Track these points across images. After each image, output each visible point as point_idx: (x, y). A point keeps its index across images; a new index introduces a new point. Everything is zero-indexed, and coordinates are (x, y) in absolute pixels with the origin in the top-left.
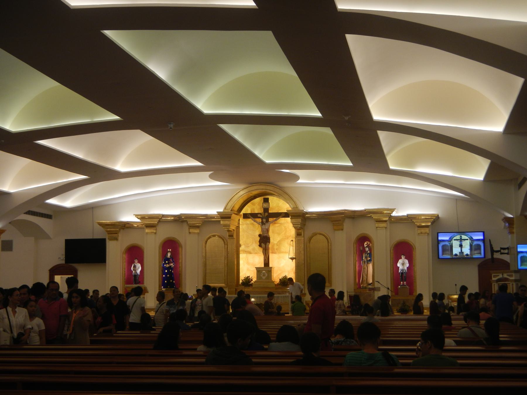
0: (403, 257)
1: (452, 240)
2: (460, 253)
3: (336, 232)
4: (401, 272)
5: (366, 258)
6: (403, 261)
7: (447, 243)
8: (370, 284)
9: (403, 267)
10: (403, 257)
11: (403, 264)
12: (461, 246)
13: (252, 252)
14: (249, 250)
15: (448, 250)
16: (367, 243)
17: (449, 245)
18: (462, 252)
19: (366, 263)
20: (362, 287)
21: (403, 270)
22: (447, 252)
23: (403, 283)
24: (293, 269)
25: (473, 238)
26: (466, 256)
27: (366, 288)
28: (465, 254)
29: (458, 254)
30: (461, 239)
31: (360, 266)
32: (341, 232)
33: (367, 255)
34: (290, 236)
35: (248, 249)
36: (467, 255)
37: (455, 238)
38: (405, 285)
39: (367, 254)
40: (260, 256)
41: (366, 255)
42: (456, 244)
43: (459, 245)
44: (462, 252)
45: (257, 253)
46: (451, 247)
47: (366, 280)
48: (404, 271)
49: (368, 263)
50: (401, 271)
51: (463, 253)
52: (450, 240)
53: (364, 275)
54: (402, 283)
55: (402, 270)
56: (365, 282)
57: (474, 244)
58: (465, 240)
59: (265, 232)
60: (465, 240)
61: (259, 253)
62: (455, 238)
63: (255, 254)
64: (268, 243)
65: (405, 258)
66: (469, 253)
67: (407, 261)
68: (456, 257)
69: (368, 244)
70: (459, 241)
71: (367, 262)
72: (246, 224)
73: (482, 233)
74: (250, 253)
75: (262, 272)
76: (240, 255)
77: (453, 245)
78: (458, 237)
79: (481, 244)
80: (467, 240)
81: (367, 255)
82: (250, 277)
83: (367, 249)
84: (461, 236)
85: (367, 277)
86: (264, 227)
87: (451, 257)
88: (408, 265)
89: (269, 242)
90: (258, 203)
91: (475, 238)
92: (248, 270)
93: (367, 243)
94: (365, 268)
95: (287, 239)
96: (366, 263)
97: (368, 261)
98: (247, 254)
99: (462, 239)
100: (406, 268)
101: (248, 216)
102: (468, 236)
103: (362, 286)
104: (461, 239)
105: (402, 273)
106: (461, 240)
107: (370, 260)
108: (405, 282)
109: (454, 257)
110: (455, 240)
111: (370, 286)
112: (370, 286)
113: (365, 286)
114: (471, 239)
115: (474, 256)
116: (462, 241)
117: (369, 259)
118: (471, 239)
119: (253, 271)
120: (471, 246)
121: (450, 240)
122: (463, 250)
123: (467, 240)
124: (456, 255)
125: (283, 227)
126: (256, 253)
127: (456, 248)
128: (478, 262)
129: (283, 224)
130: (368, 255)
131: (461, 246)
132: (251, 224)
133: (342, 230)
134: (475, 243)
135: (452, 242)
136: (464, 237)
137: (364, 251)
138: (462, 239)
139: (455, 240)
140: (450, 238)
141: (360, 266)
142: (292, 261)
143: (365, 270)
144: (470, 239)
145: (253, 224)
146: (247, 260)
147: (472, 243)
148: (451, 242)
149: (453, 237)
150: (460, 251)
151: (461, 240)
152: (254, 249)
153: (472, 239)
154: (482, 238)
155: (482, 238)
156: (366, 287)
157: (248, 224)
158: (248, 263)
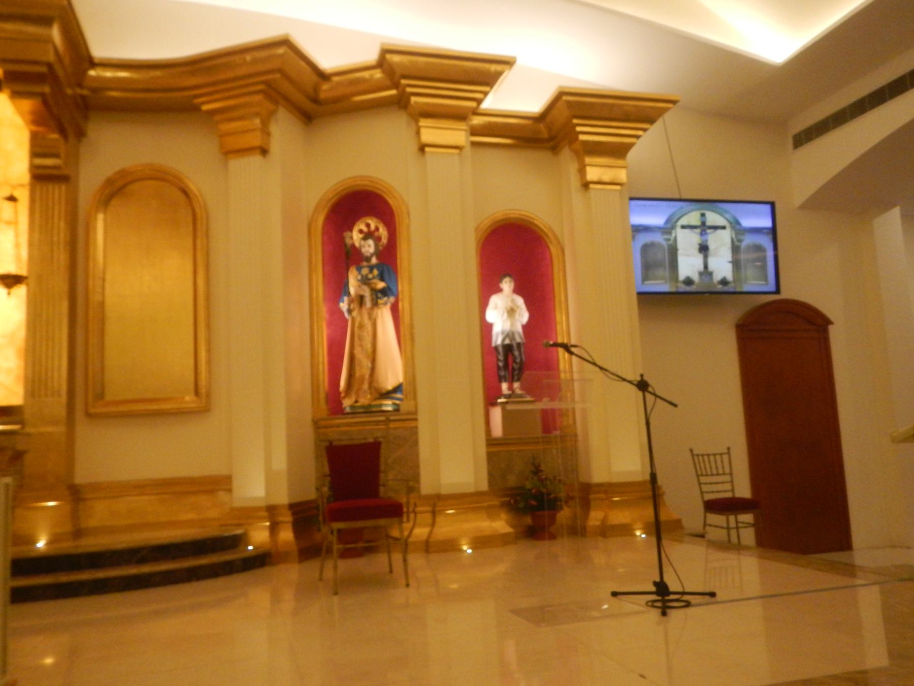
0: (507, 285)
1: (673, 227)
2: (701, 274)
3: (237, 165)
4: (507, 342)
5: (365, 281)
6: (513, 301)
7: (659, 238)
8: (387, 395)
9: (512, 325)
10: (507, 285)
11: (511, 312)
12: (704, 249)
15: (658, 265)
17: (665, 244)
18: (706, 272)
19: (368, 303)
20: (352, 407)
21: (513, 334)
22: (660, 272)
23: (510, 388)
25: (738, 223)
26: (720, 286)
27: (368, 410)
28: (717, 277)
29: (696, 278)
30: (703, 223)
31: (338, 322)
32: (256, 160)
33: (371, 271)
36: (724, 282)
37: (684, 221)
38: (520, 396)
39: (371, 268)
41: (365, 271)
42: (687, 241)
43: (697, 247)
44: (706, 272)
46: (673, 251)
47: (367, 376)
48: (518, 340)
49: (375, 304)
50: (504, 340)
51: (711, 274)
52: (668, 229)
53: (358, 351)
54: (504, 386)
55: (510, 335)
56: (366, 386)
57: (744, 245)
58: (715, 228)
60: (715, 228)
62: (684, 221)
65: (518, 290)
66: (729, 277)
67: (520, 301)
68: (688, 289)
69: (373, 227)
70: (698, 231)
71: (372, 300)
73: (767, 208)
77: (680, 245)
78: (693, 218)
79: (766, 242)
80: (724, 228)
81: (371, 271)
83: (369, 248)
84: (703, 215)
85: (374, 361)
87: (673, 290)
88: (524, 317)
91: (748, 222)
93: (368, 225)
94: (361, 326)
96: (368, 303)
97: (379, 295)
99: (709, 223)
100: (520, 329)
102: (727, 216)
103: (347, 403)
104: (703, 223)
105: (508, 349)
106: (704, 228)
107: (385, 292)
108: (516, 385)
109: (683, 288)
110: (683, 227)
111: (388, 405)
112: (388, 405)
113: (364, 400)
114: (735, 224)
115: (746, 288)
116: (709, 231)
117: (381, 285)
118: (735, 224)
120: (735, 249)
121: (668, 229)
122: (713, 263)
123: (724, 228)
124: (689, 281)
127: (688, 255)
128: (734, 313)
130: (376, 272)
131: (704, 249)
133: (264, 151)
134: (748, 240)
135: (673, 235)
136: (713, 218)
137: (353, 257)
138: (709, 223)
139: (683, 227)
140: (667, 221)
141: (338, 322)
142: (9, 294)
143: (365, 334)
144: (733, 228)
147: (740, 241)
148: (670, 233)
149: (679, 219)
150: (701, 267)
151: (704, 228)
153: (738, 227)
154: (767, 223)
155: (767, 223)
156: (370, 405)
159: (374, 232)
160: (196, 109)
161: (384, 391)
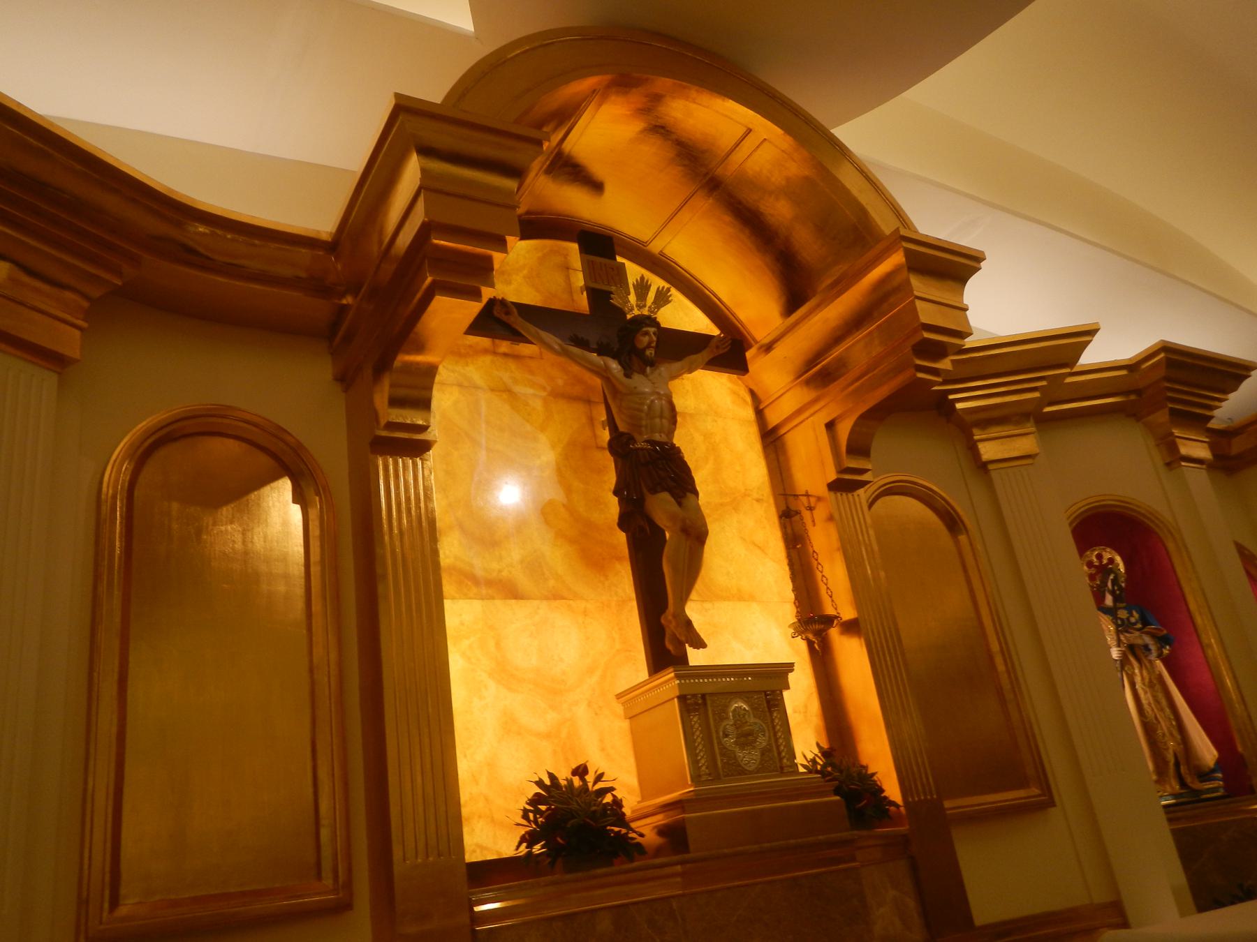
13: (523, 581)
14: (505, 573)
16: (1099, 557)
24: (806, 707)
34: (746, 495)
35: (495, 566)
40: (585, 613)
45: (563, 598)
59: (661, 417)
61: (576, 596)
63: (547, 598)
64: (690, 496)
72: (460, 385)
74: (511, 592)
75: (721, 715)
76: (447, 604)
82: (590, 778)
86: (640, 383)
89: (696, 493)
90: (525, 272)
92: (510, 726)
95: (736, 509)
98: (492, 598)
101: (504, 318)
119: (548, 736)
125: (698, 438)
126: (555, 596)
129: (691, 415)
132: (492, 390)
145: (505, 391)
146: (498, 645)
152: (535, 566)
157: (477, 387)
158: (505, 674)
159: (1107, 564)
160: (943, 406)
161: (1207, 770)
